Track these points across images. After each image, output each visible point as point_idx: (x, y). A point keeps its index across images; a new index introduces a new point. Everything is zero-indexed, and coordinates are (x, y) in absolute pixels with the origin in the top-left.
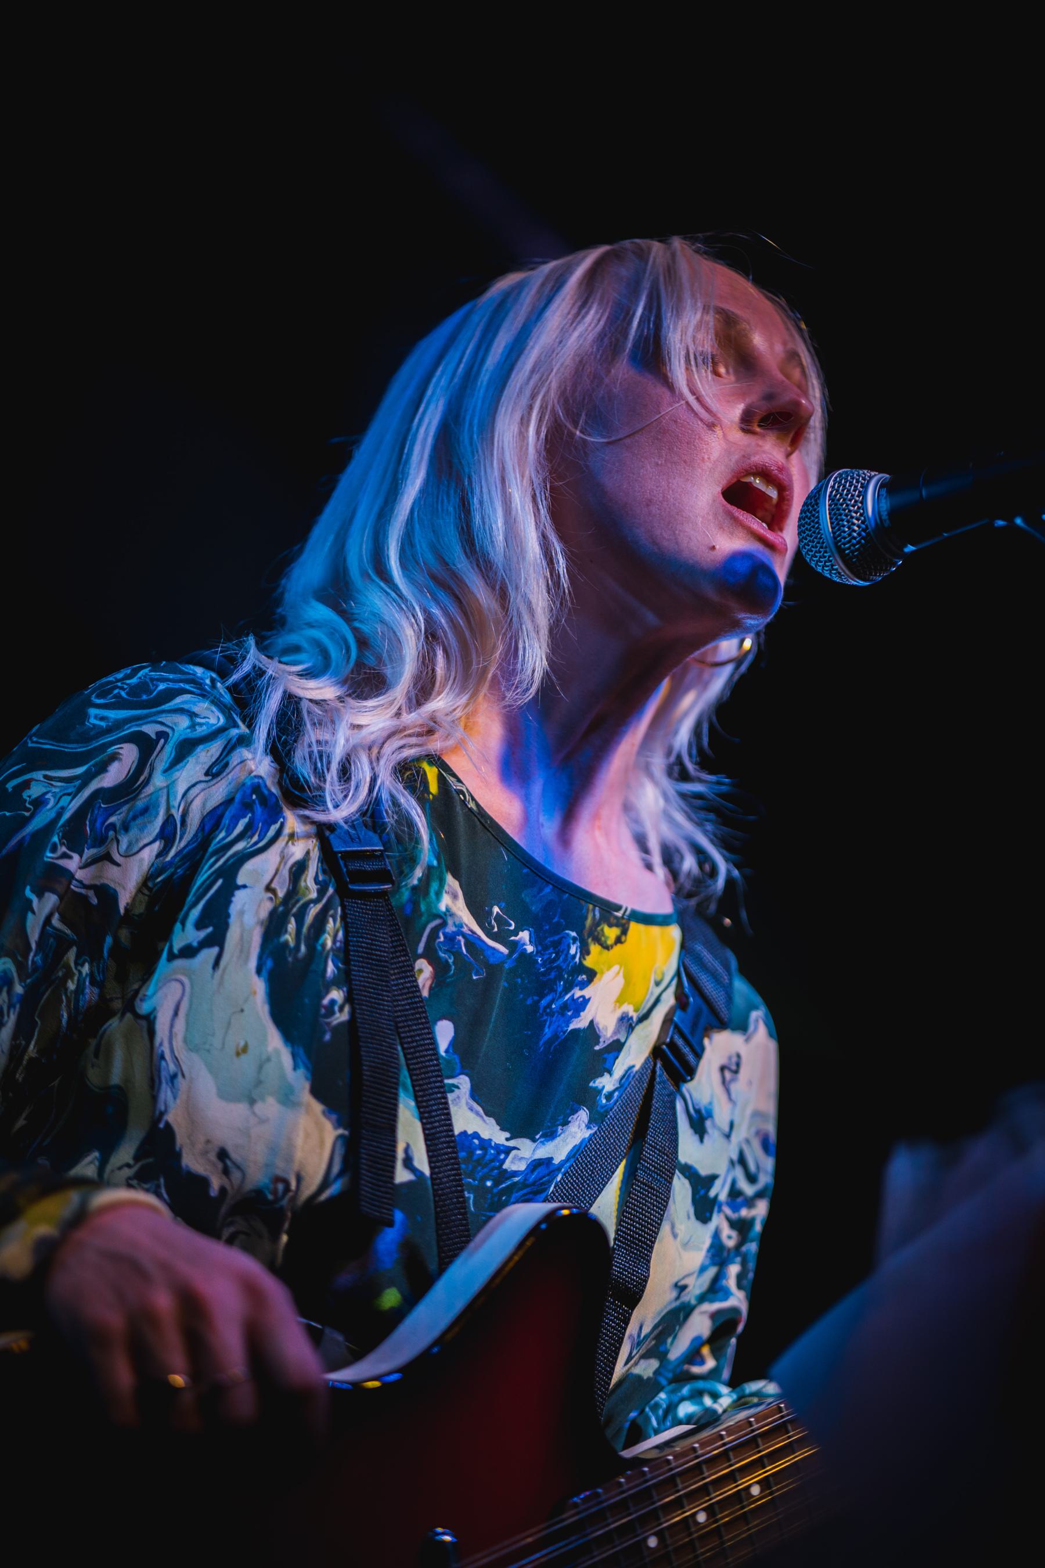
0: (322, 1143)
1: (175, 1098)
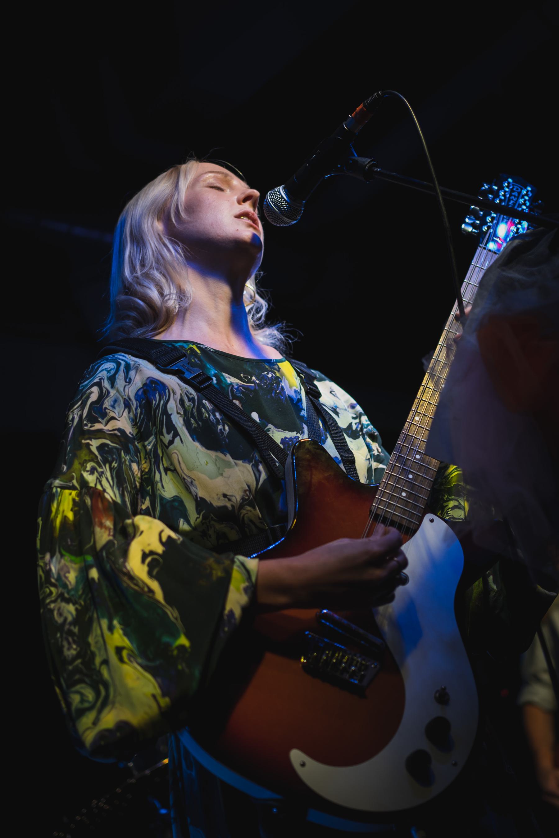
0: (249, 471)
1: (197, 488)
